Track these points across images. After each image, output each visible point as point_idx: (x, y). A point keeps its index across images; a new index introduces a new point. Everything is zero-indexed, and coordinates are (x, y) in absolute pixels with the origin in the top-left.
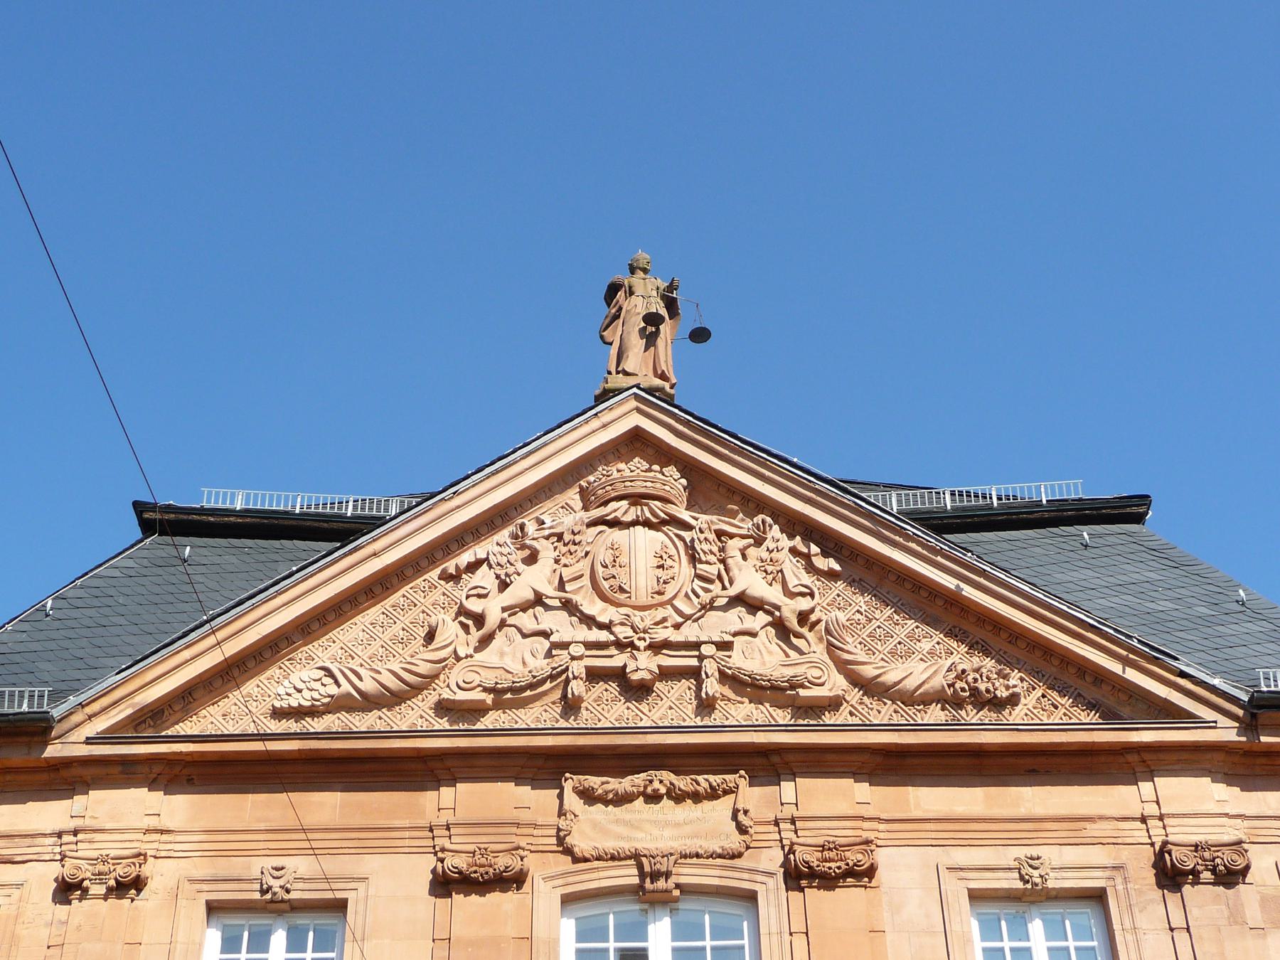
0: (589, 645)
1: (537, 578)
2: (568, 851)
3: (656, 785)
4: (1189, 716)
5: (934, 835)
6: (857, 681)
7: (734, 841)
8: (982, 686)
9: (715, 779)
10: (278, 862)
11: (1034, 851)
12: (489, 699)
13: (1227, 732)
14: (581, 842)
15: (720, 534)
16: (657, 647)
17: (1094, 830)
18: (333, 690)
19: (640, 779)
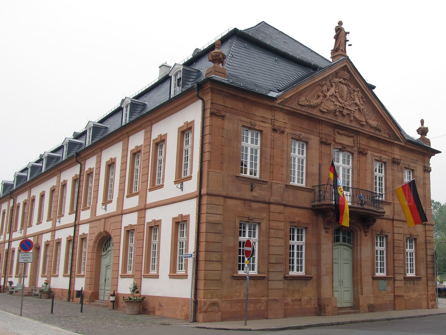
2: (335, 141)
6: (366, 122)
7: (353, 145)
9: (352, 135)
10: (301, 133)
12: (326, 111)
13: (403, 144)
14: (337, 141)
15: (354, 90)
17: (388, 153)
18: (307, 103)
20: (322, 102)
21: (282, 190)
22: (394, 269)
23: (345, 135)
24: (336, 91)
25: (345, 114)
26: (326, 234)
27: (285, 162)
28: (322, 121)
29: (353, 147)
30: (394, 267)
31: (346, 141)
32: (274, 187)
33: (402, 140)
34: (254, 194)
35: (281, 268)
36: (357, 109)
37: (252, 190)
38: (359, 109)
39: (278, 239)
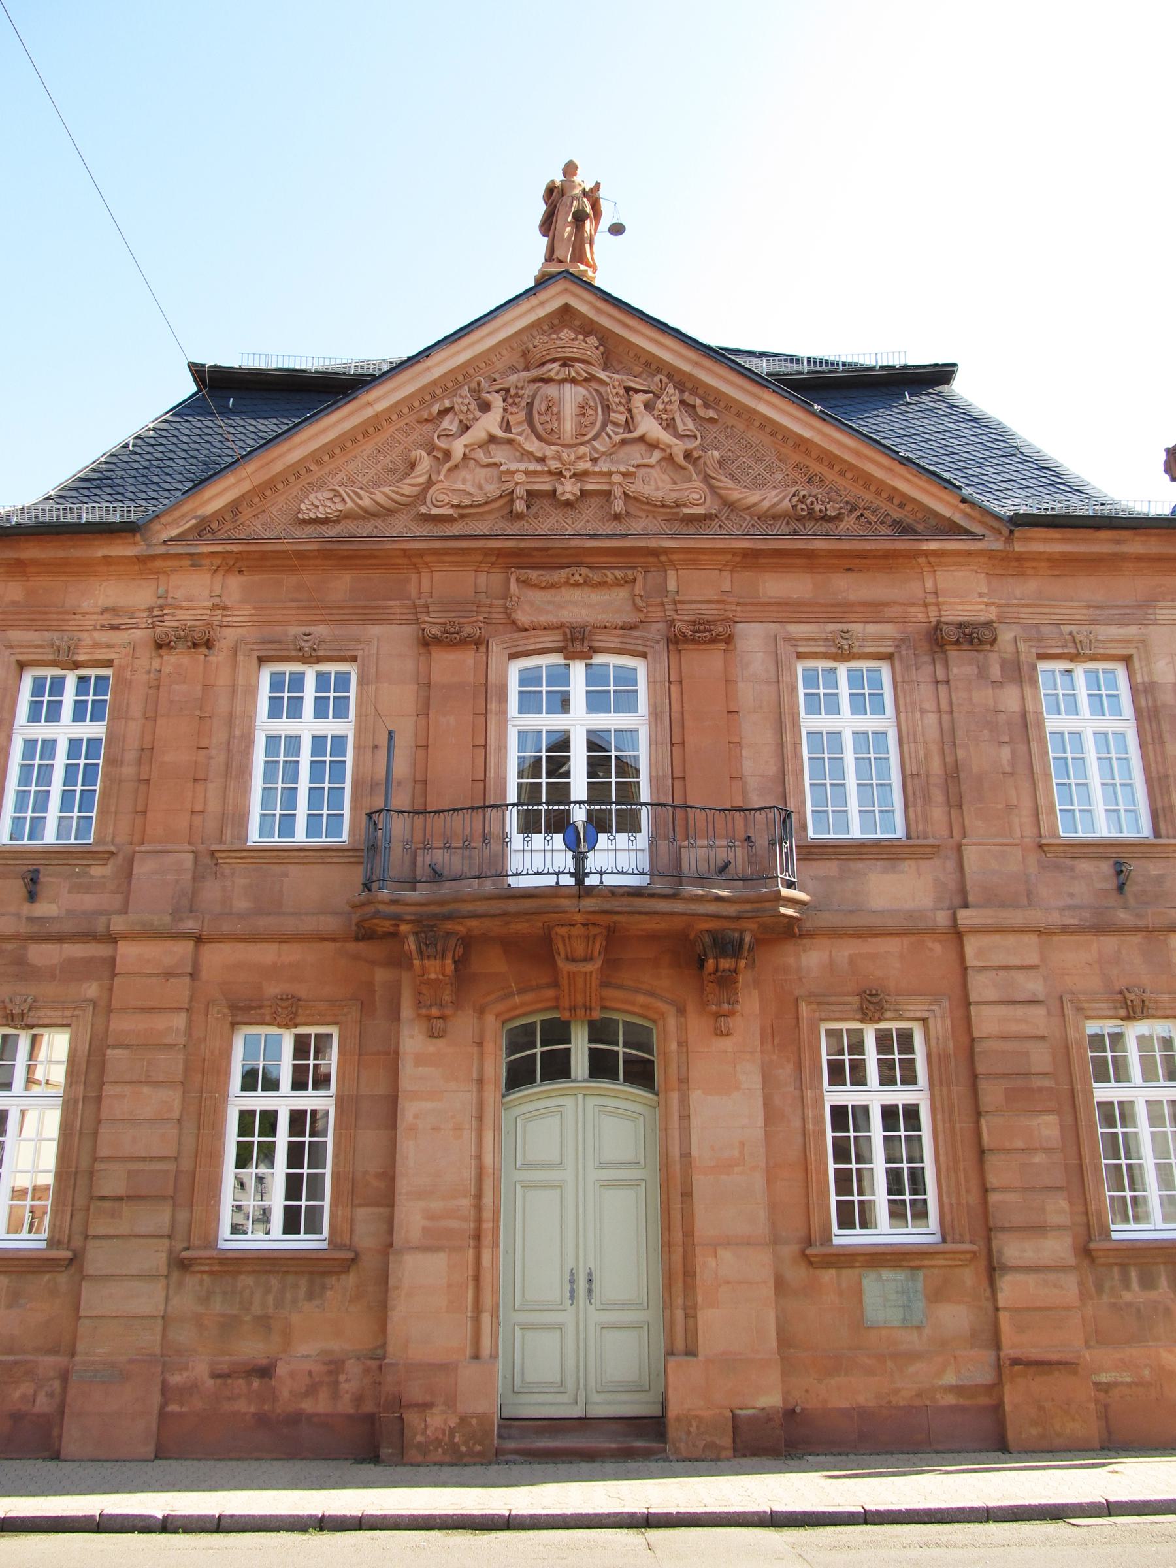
0: (526, 473)
1: (490, 423)
2: (514, 623)
3: (577, 577)
4: (967, 532)
5: (775, 615)
7: (632, 618)
8: (817, 507)
10: (307, 629)
11: (845, 627)
15: (628, 389)
16: (579, 476)
18: (340, 506)
19: (564, 573)
20: (430, 483)
21: (188, 876)
22: (985, 1202)
23: (577, 585)
24: (512, 420)
25: (569, 496)
26: (432, 1047)
27: (219, 759)
28: (421, 553)
29: (632, 627)
30: (985, 1191)
31: (581, 606)
32: (142, 869)
33: (976, 528)
34: (44, 908)
35: (158, 1218)
36: (653, 461)
37: (32, 897)
38: (670, 459)
39: (146, 1090)
